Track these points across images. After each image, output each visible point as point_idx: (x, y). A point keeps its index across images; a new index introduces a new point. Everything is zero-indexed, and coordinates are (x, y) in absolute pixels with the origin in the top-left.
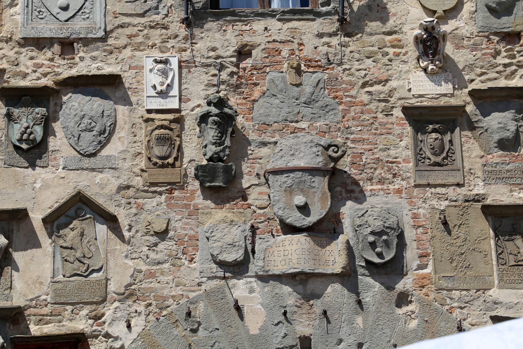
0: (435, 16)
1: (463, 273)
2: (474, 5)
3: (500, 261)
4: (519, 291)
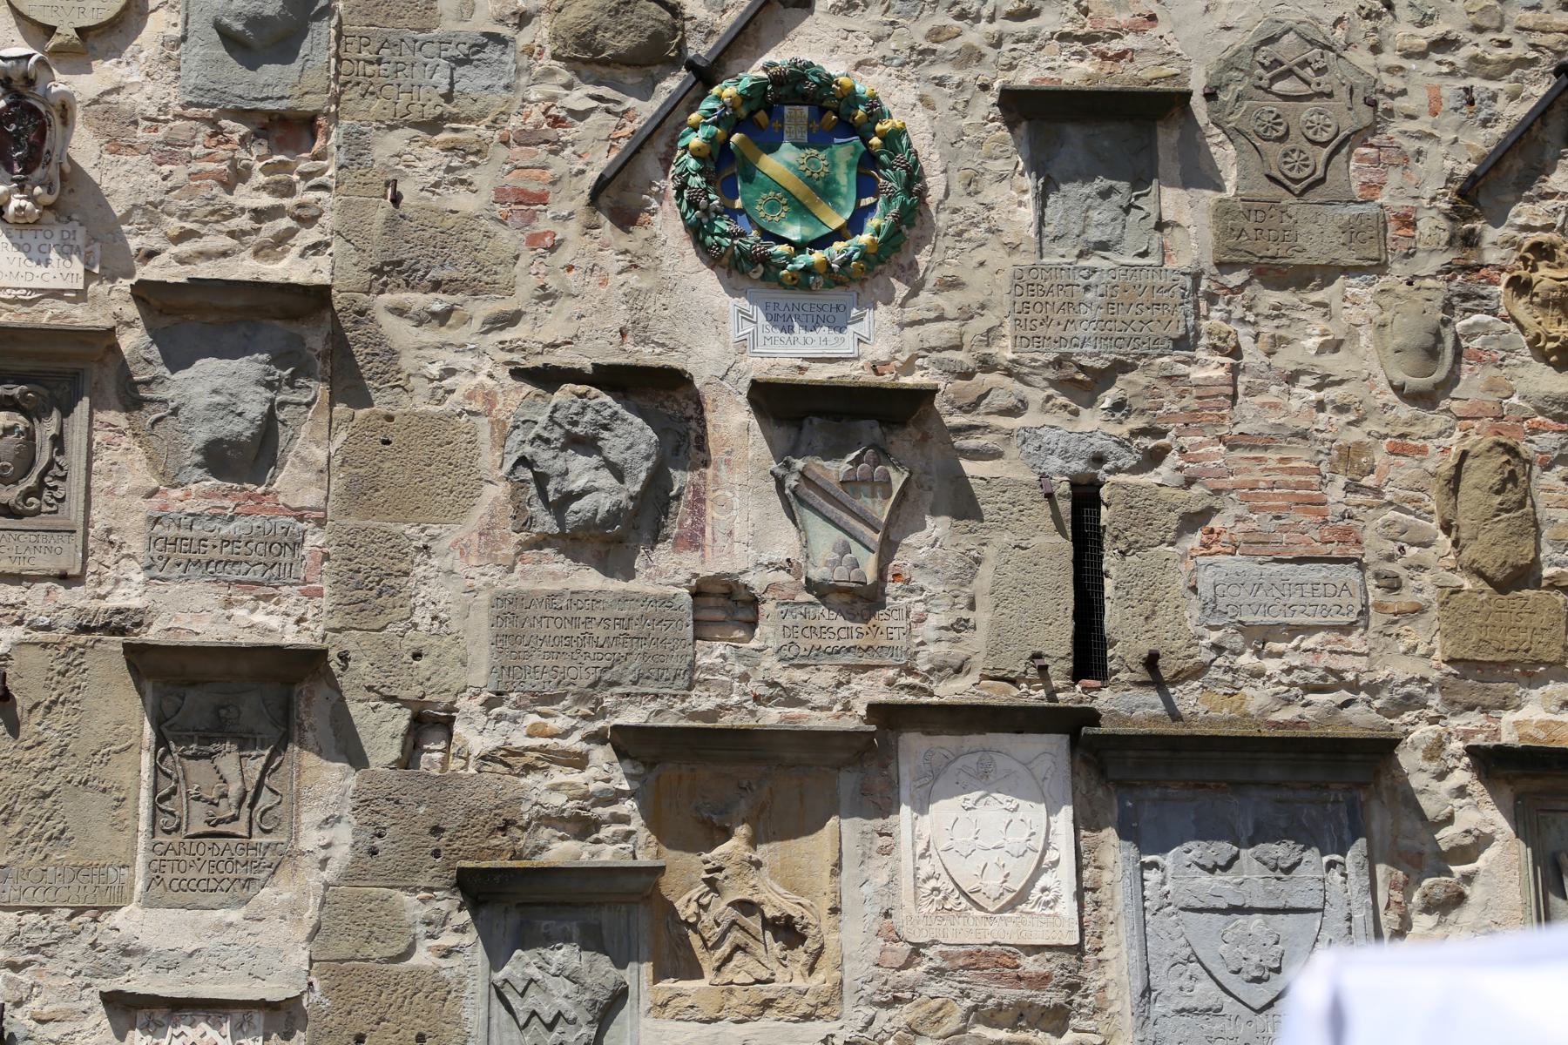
0: (51, 44)
1: (38, 857)
2: (179, 20)
3: (162, 820)
4: (207, 914)
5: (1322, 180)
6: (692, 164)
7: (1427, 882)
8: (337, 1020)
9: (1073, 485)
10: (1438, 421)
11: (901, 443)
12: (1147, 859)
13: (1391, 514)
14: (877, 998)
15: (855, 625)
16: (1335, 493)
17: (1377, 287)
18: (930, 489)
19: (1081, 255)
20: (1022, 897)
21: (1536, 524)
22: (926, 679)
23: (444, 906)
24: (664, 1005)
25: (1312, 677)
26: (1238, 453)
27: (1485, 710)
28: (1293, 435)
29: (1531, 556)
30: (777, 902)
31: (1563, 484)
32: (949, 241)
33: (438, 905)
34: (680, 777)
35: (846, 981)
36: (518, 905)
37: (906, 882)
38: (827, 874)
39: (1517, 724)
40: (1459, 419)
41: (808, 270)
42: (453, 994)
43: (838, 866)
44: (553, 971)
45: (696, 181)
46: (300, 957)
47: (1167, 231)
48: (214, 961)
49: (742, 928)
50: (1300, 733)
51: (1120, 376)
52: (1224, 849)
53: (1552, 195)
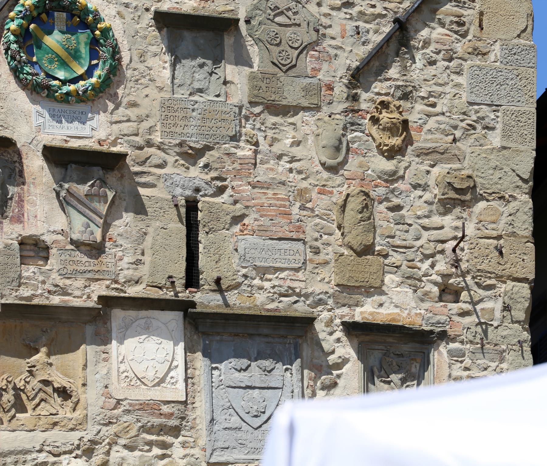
5: (295, 66)
6: (12, 38)
7: (323, 377)
9: (187, 201)
10: (338, 180)
11: (112, 178)
12: (214, 365)
13: (318, 220)
14: (102, 422)
15: (92, 261)
16: (295, 210)
17: (316, 117)
18: (125, 200)
19: (191, 94)
20: (162, 380)
21: (374, 227)
22: (123, 286)
25: (283, 290)
26: (256, 190)
27: (350, 306)
28: (279, 183)
29: (372, 241)
30: (59, 381)
31: (386, 210)
32: (132, 84)
34: (16, 326)
35: (89, 415)
37: (114, 373)
38: (81, 369)
39: (361, 313)
40: (347, 179)
41: (68, 94)
43: (85, 366)
45: (14, 46)
47: (228, 85)
49: (44, 392)
50: (277, 314)
51: (207, 152)
52: (244, 362)
53: (389, 79)
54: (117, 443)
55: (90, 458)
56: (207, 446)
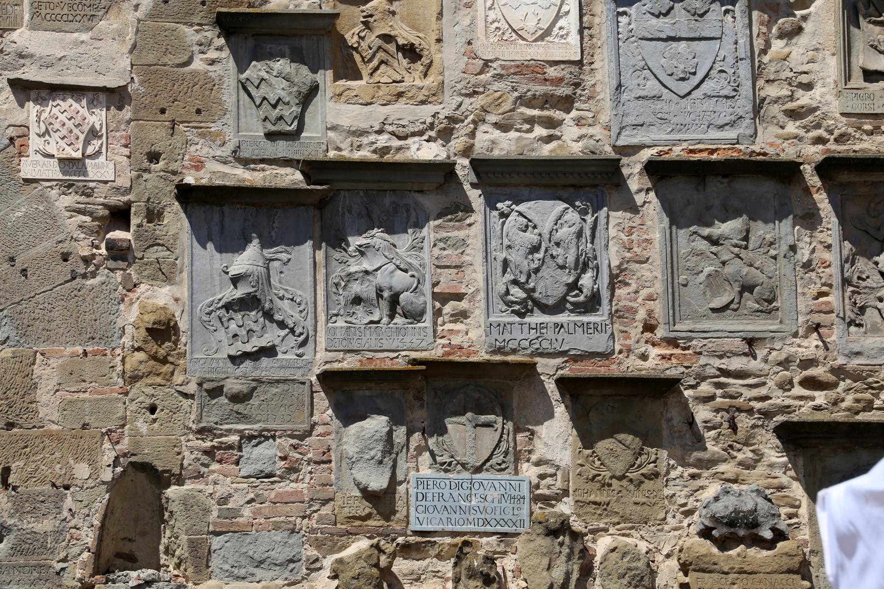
4: (68, 35)
7: (781, 21)
8: (149, 100)
12: (621, 10)
14: (463, 91)
20: (548, 32)
23: (209, 34)
24: (340, 95)
30: (405, 35)
33: (206, 34)
36: (253, 35)
37: (481, 24)
38: (434, 19)
42: (217, 86)
43: (440, 15)
44: (275, 74)
46: (125, 62)
48: (74, 63)
49: (385, 50)
54: (484, 120)
55: (448, 141)
56: (612, 123)
